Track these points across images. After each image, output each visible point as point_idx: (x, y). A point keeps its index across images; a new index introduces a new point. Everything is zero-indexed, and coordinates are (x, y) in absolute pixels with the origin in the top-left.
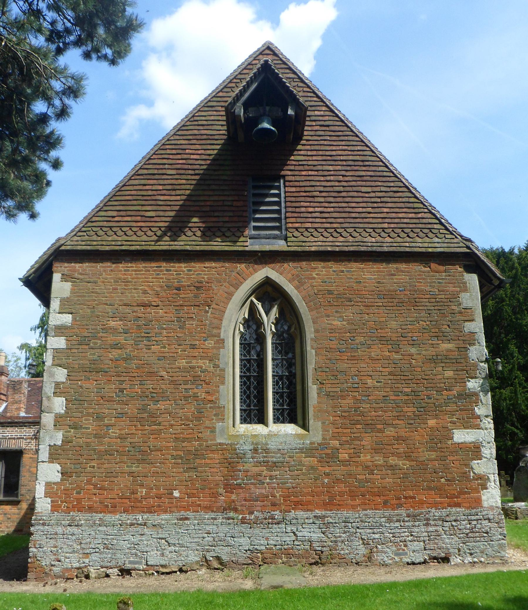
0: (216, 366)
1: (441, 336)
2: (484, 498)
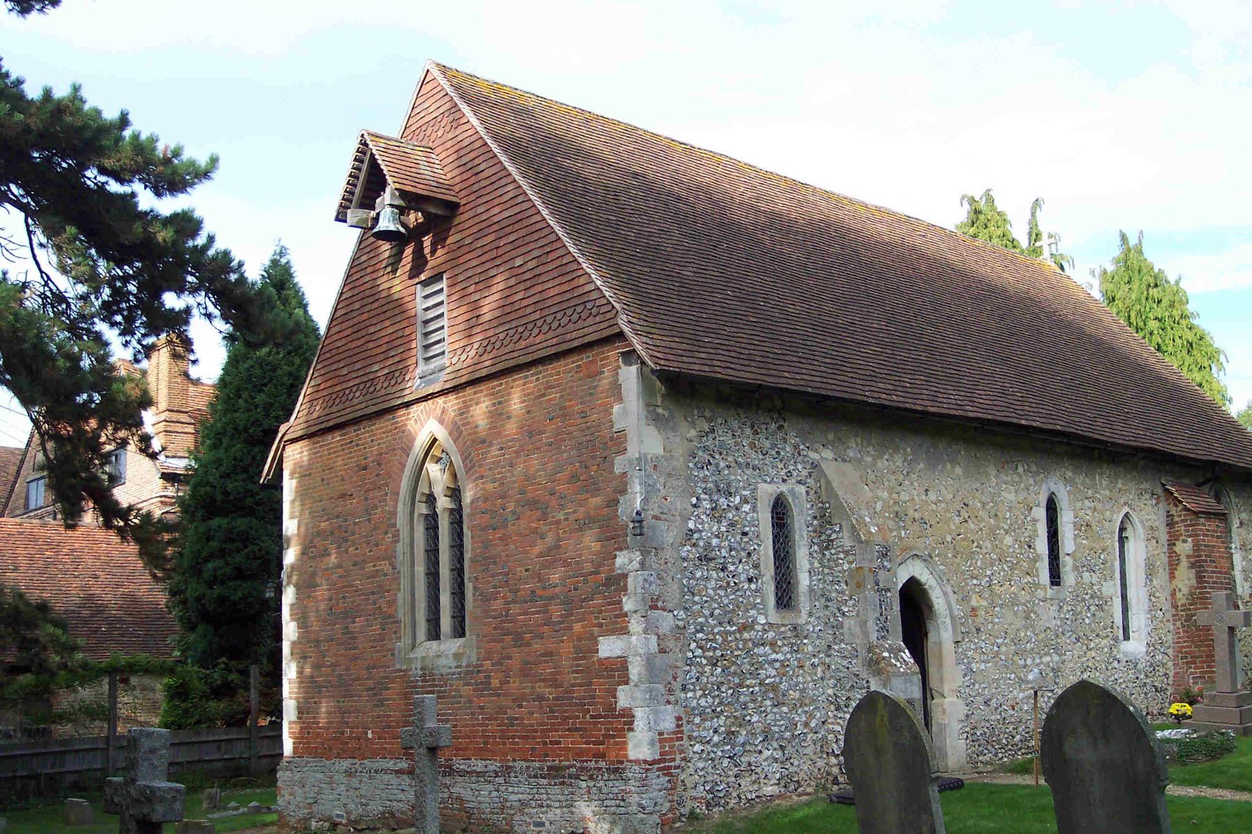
0: (394, 568)
1: (592, 488)
2: (630, 746)
